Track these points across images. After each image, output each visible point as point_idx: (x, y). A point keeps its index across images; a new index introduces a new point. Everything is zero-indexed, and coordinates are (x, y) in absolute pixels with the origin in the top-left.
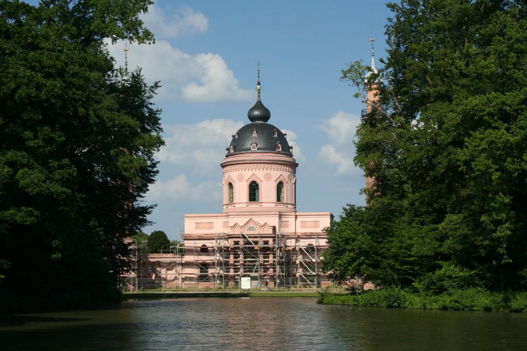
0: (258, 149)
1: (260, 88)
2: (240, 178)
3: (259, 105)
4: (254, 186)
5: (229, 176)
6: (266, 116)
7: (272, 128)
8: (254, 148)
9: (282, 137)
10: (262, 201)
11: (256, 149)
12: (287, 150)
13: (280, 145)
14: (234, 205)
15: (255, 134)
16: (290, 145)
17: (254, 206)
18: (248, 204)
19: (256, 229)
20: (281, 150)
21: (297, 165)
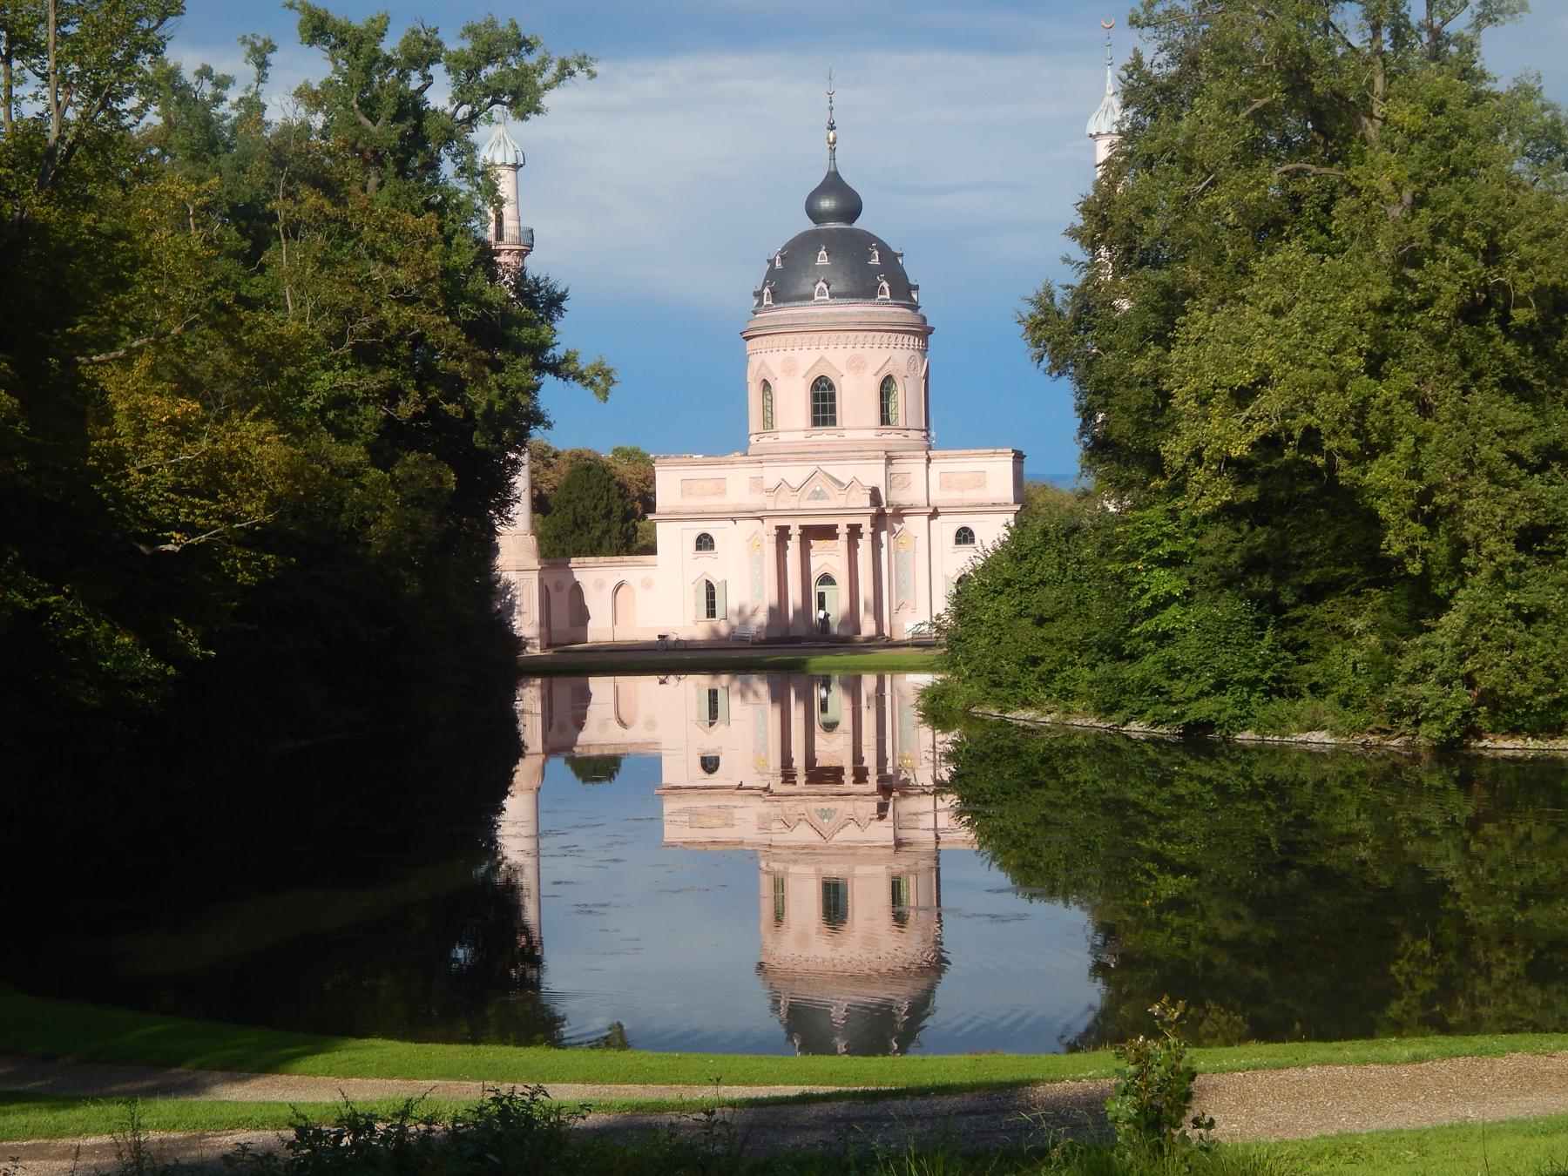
0: (832, 296)
1: (835, 139)
2: (790, 369)
3: (833, 183)
4: (824, 389)
5: (763, 363)
6: (851, 208)
7: (866, 241)
8: (821, 293)
9: (891, 260)
10: (844, 425)
11: (827, 297)
12: (903, 291)
13: (885, 284)
14: (775, 435)
15: (823, 259)
16: (912, 282)
17: (824, 435)
18: (809, 434)
19: (830, 496)
20: (888, 296)
21: (930, 331)
